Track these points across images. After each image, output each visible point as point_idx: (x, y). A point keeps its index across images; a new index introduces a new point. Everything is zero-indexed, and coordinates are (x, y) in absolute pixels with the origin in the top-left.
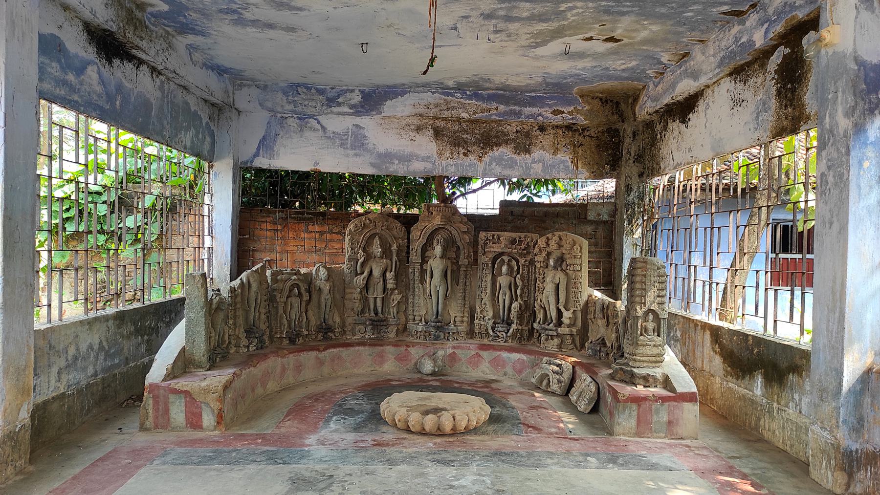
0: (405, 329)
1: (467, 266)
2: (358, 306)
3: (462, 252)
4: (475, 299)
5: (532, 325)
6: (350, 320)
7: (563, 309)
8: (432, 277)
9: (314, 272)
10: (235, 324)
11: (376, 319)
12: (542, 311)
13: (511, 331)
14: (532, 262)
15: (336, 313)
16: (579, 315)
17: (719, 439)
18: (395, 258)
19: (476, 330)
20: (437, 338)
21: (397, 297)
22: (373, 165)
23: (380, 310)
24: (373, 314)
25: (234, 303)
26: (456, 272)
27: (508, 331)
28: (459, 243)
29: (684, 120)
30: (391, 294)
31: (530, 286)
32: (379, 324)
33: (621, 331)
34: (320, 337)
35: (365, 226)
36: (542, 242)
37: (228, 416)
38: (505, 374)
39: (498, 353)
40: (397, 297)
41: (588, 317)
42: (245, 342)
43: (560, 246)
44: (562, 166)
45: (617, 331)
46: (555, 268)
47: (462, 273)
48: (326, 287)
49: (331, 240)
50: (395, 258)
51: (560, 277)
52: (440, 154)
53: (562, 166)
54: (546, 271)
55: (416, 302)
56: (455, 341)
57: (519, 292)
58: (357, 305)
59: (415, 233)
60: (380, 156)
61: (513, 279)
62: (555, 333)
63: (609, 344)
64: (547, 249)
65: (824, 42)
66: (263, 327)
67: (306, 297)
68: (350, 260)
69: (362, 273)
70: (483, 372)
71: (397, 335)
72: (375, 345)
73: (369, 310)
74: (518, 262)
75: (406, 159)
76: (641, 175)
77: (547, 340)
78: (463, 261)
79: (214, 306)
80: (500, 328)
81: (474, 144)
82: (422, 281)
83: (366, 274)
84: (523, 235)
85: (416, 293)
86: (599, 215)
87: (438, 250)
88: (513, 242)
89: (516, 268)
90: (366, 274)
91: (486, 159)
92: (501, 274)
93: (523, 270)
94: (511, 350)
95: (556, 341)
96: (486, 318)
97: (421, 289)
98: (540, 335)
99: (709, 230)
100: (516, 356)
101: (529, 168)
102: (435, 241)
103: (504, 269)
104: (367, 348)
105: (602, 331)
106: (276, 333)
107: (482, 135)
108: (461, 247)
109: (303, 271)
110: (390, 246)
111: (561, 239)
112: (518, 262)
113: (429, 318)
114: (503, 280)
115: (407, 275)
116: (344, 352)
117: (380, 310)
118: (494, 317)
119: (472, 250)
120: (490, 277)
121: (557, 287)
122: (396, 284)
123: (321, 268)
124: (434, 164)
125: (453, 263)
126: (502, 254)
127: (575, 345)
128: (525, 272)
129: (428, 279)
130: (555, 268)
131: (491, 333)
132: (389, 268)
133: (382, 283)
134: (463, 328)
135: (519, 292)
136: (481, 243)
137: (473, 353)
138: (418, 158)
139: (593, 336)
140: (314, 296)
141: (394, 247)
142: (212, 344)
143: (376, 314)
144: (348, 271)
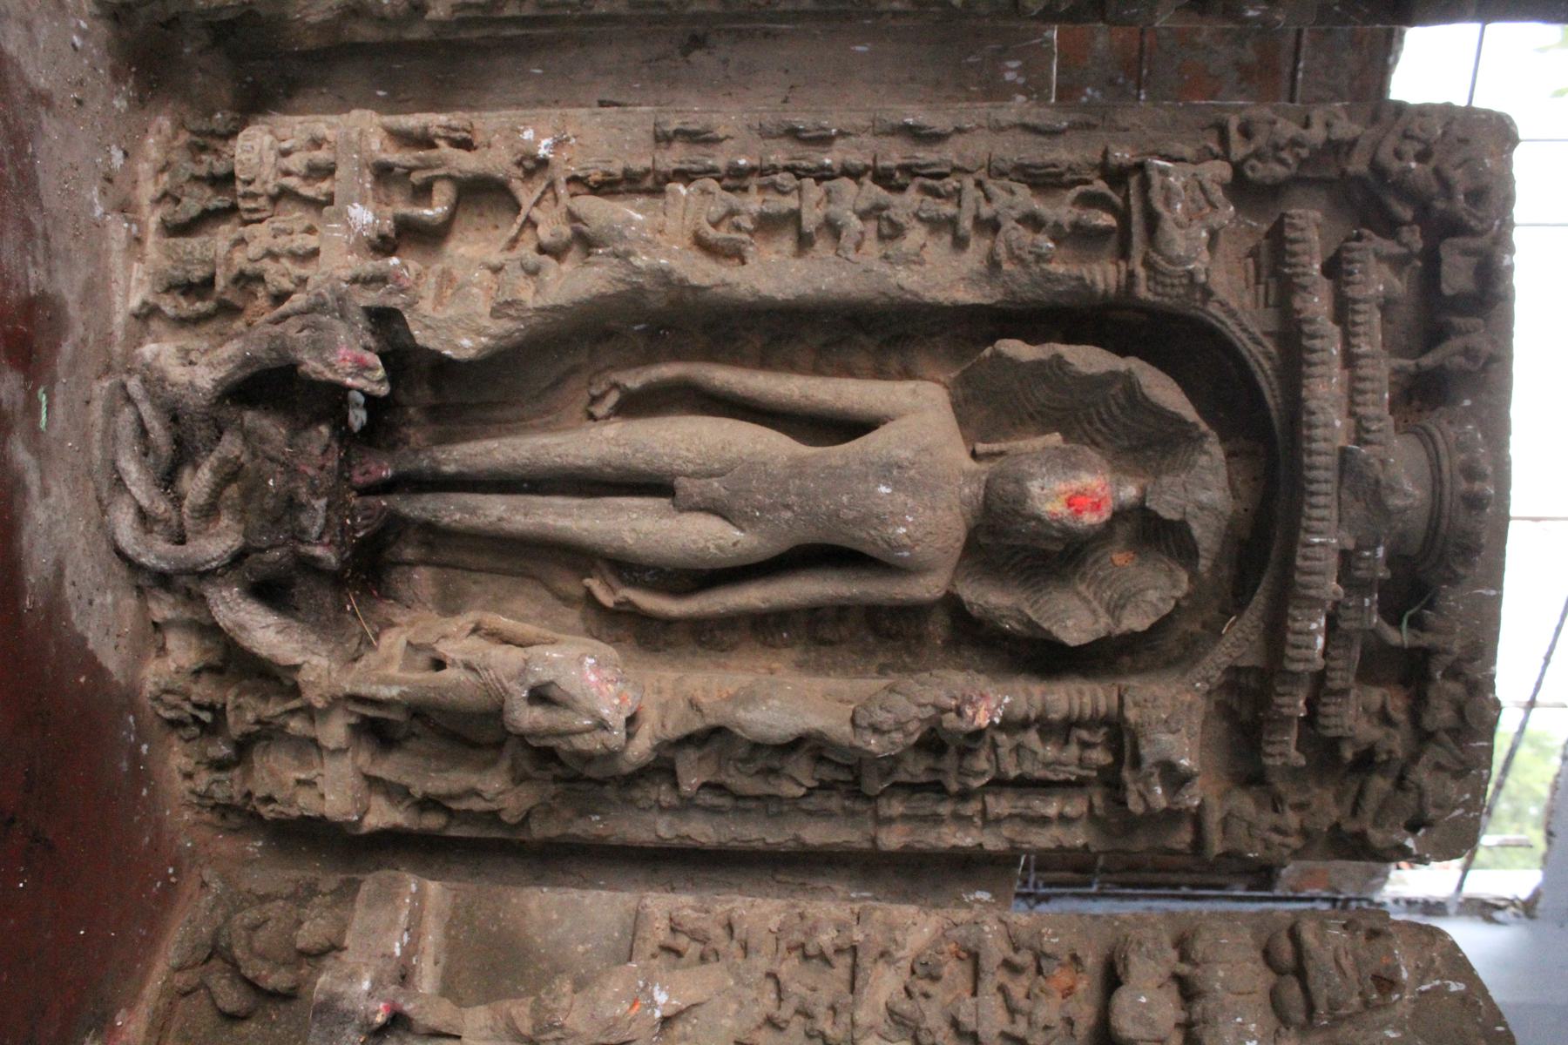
13: (265, 632)
19: (258, 149)
61: (927, 588)
92: (988, 408)
93: (1060, 730)
103: (1069, 487)
120: (942, 275)
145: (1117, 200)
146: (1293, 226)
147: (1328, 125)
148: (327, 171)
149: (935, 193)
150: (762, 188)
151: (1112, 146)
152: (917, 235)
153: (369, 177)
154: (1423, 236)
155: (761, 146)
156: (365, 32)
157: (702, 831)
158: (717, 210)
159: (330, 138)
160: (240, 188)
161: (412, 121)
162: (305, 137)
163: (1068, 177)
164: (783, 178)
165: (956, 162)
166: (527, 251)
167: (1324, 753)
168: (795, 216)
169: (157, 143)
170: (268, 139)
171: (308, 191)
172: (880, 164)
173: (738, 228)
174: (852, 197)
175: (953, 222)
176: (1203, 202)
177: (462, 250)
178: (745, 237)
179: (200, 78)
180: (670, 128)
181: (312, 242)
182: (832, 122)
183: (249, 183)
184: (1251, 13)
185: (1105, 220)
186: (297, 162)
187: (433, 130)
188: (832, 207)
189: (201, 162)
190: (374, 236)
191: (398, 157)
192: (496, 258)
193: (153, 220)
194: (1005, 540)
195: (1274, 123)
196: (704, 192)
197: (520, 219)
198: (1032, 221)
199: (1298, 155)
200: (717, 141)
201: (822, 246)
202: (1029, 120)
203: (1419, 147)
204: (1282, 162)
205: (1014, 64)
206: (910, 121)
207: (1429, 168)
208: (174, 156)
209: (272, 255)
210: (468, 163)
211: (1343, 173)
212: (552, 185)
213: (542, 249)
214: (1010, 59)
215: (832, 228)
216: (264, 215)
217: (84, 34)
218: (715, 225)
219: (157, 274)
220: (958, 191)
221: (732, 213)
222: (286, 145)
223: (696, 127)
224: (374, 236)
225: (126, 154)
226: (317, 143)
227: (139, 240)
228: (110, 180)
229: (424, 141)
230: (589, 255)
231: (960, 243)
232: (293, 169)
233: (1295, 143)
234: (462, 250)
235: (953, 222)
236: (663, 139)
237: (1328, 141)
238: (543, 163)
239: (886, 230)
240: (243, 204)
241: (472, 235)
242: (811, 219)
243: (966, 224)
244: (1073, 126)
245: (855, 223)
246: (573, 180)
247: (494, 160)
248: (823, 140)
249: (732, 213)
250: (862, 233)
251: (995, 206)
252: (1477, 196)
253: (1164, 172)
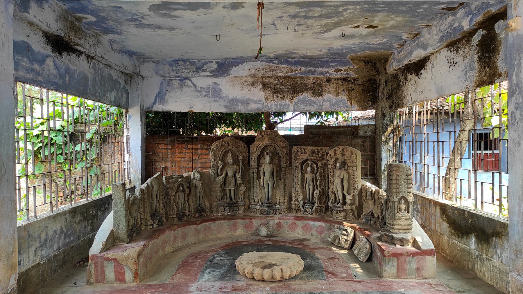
0: (249, 207)
1: (285, 168)
2: (219, 195)
3: (282, 160)
4: (291, 187)
5: (327, 204)
6: (215, 204)
7: (346, 194)
8: (264, 175)
9: (192, 175)
10: (144, 211)
11: (231, 202)
12: (333, 195)
13: (314, 208)
14: (326, 165)
15: (206, 200)
16: (357, 197)
17: (449, 278)
18: (241, 165)
19: (293, 207)
20: (269, 213)
21: (243, 188)
22: (226, 107)
23: (233, 197)
24: (229, 200)
25: (143, 199)
26: (279, 172)
27: (313, 207)
28: (280, 154)
29: (418, 74)
30: (240, 187)
31: (325, 180)
32: (232, 205)
33: (384, 208)
34: (197, 215)
35: (222, 146)
36: (331, 152)
37: (141, 273)
38: (312, 235)
39: (307, 222)
40: (243, 188)
41: (362, 199)
42: (150, 222)
43: (343, 155)
44: (342, 103)
45: (381, 208)
46: (340, 168)
47: (282, 172)
48: (200, 185)
49: (202, 154)
50: (241, 165)
51: (344, 174)
52: (267, 98)
53: (342, 103)
54: (335, 170)
55: (255, 191)
56: (280, 215)
57: (318, 183)
58: (219, 194)
59: (253, 148)
60: (230, 101)
61: (314, 176)
62: (342, 209)
63: (376, 216)
64: (335, 157)
65: (511, 29)
66: (162, 211)
67: (187, 192)
68: (213, 167)
69: (221, 175)
70: (298, 234)
71: (244, 212)
72: (231, 219)
73: (227, 197)
74: (317, 165)
75: (245, 102)
76: (391, 107)
77: (337, 213)
78: (283, 165)
79: (131, 202)
80: (307, 206)
81: (287, 92)
82: (258, 178)
83: (223, 175)
84: (319, 148)
86: (366, 132)
87: (267, 159)
88: (313, 152)
89: (316, 169)
90: (223, 175)
91: (295, 100)
92: (307, 173)
93: (321, 170)
94: (315, 220)
95: (343, 214)
96: (299, 200)
97: (258, 183)
98: (332, 210)
99: (436, 143)
100: (318, 224)
101: (321, 105)
102: (266, 154)
103: (309, 169)
104: (226, 221)
105: (371, 208)
106: (170, 215)
107: (292, 86)
108: (282, 157)
109: (185, 175)
110: (238, 157)
111: (343, 151)
112: (317, 165)
113: (263, 201)
114: (308, 176)
116: (212, 224)
117: (233, 197)
118: (303, 199)
119: (288, 158)
120: (300, 174)
121: (342, 180)
122: (243, 181)
123: (196, 173)
124: (263, 105)
125: (277, 167)
126: (307, 160)
127: (355, 216)
128: (322, 171)
129: (262, 177)
130: (340, 168)
131: (302, 209)
132: (238, 171)
133: (233, 180)
134: (285, 206)
135: (318, 183)
136: (294, 153)
137: (291, 222)
138: (253, 101)
139: (366, 211)
140: (193, 191)
141: (241, 158)
142: (130, 226)
143: (231, 199)
144: (212, 174)
157: (327, 187)
167: (321, 157)
174: (296, 178)
194: (313, 171)
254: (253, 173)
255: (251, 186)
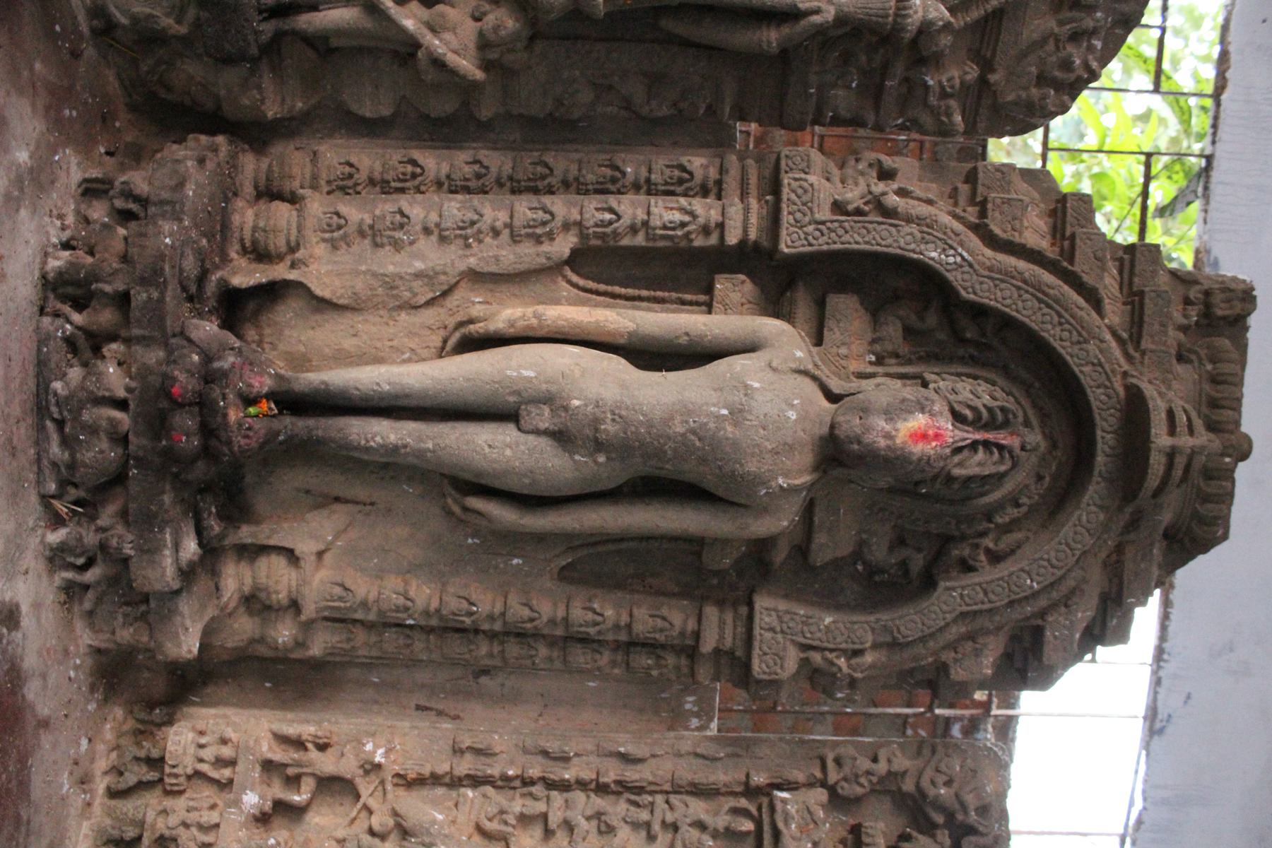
19: (182, 740)
28: (953, 595)
47: (678, 617)
55: (417, 209)
82: (606, 264)
85: (492, 211)
87: (918, 420)
97: (529, 254)
102: (978, 392)
108: (910, 620)
115: (646, 130)
145: (754, 810)
146: (867, 834)
147: (889, 761)
148: (232, 763)
149: (637, 804)
150: (523, 795)
151: (752, 773)
152: (624, 832)
153: (258, 768)
154: (950, 837)
155: (522, 759)
156: (262, 650)
158: (492, 810)
159: (235, 740)
160: (167, 770)
161: (291, 730)
162: (217, 736)
163: (723, 790)
164: (538, 789)
165: (651, 778)
166: (362, 825)
168: (544, 817)
169: (112, 728)
170: (191, 735)
171: (215, 774)
172: (601, 780)
173: (506, 823)
175: (648, 825)
176: (809, 819)
177: (317, 820)
178: (510, 829)
179: (146, 675)
180: (464, 746)
181: (214, 817)
182: (571, 750)
183: (174, 767)
184: (839, 695)
185: (748, 826)
186: (208, 754)
187: (304, 737)
188: (569, 813)
189: (143, 747)
190: (257, 813)
191: (279, 755)
192: (340, 834)
193: (101, 785)
195: (856, 759)
196: (485, 796)
197: (359, 805)
198: (701, 826)
199: (870, 781)
200: (495, 754)
201: (561, 838)
202: (699, 751)
203: (945, 778)
204: (862, 786)
205: (690, 699)
206: (622, 750)
207: (952, 791)
208: (123, 742)
209: (186, 825)
210: (327, 764)
211: (900, 789)
212: (382, 782)
213: (372, 832)
214: (689, 695)
215: (569, 826)
216: (182, 788)
217: (76, 668)
218: (490, 820)
219: (100, 831)
220: (652, 804)
221: (502, 812)
222: (203, 741)
223: (480, 746)
224: (257, 813)
225: (90, 740)
226: (224, 741)
227: (89, 804)
228: (76, 764)
229: (298, 744)
230: (404, 839)
231: (651, 838)
232: (206, 758)
233: (868, 773)
234: (317, 820)
235: (648, 825)
236: (458, 751)
237: (890, 773)
238: (379, 766)
239: (603, 828)
240: (167, 780)
241: (324, 810)
242: (554, 819)
243: (656, 827)
244: (728, 756)
245: (583, 822)
246: (398, 775)
247: (347, 766)
248: (565, 759)
249: (502, 812)
250: (587, 832)
251: (676, 815)
252: (983, 810)
253: (784, 801)
254: (680, 185)
255: (498, 162)
